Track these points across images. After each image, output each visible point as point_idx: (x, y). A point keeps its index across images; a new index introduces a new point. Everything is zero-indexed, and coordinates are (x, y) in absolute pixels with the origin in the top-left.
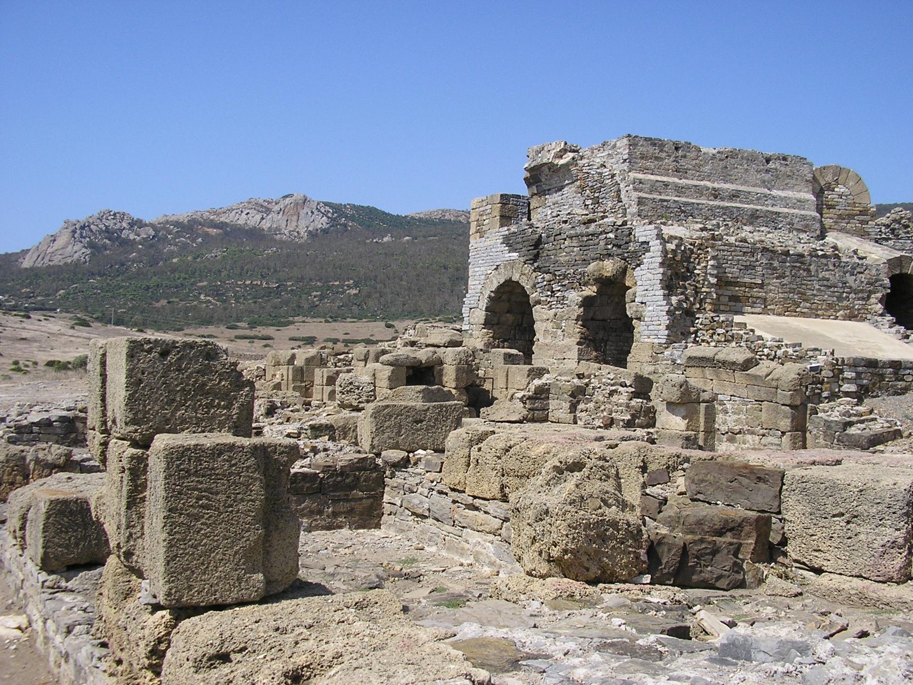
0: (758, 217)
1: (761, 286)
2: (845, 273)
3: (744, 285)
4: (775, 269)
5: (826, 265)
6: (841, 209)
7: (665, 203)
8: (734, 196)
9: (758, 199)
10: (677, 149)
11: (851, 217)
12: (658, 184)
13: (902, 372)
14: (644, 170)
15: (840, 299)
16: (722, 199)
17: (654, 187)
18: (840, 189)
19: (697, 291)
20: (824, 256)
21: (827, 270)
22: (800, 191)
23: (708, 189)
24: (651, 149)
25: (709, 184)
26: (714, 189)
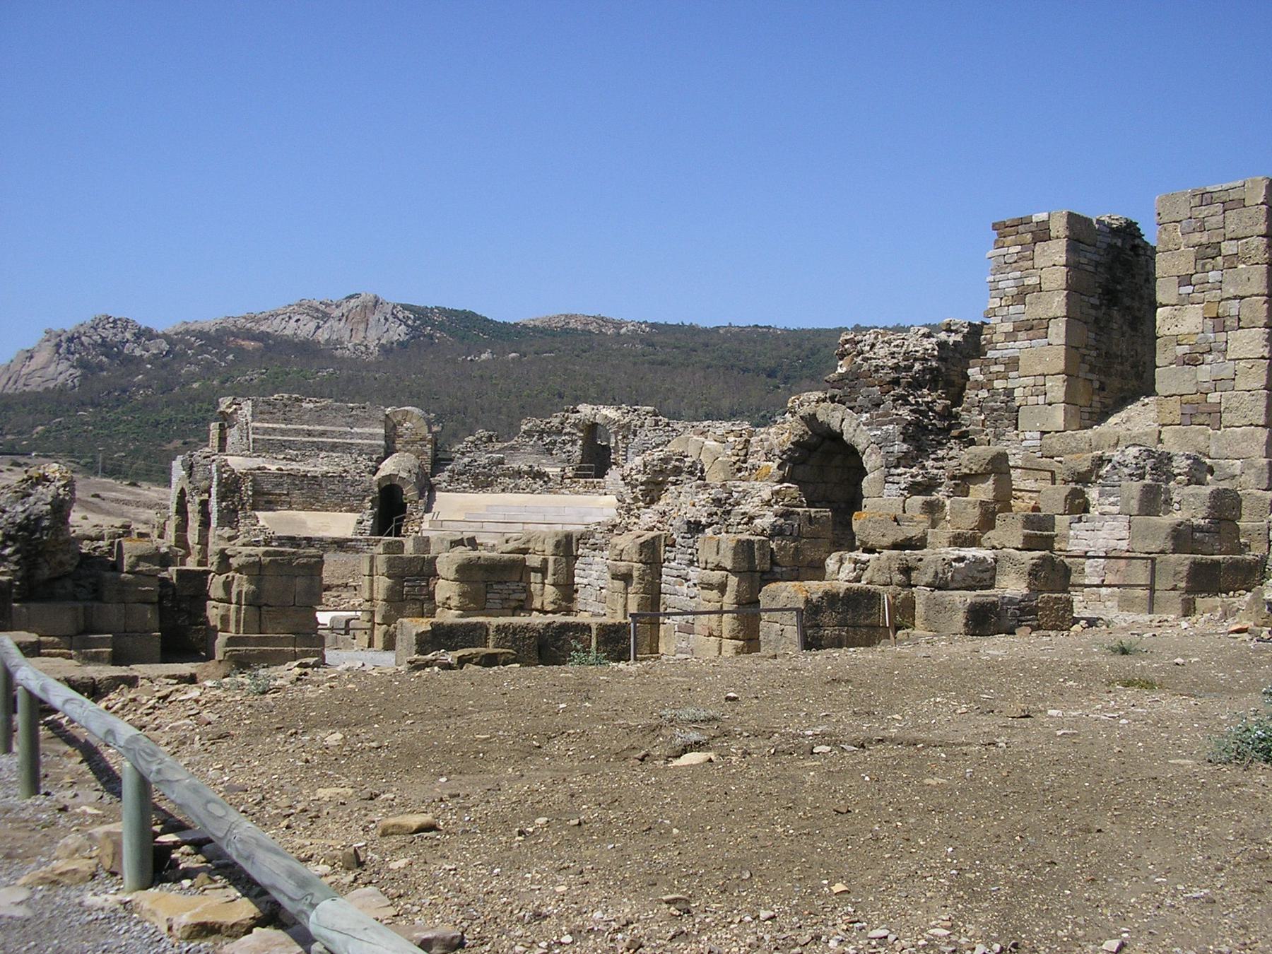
6: (406, 438)
8: (323, 434)
11: (414, 442)
14: (261, 421)
15: (343, 500)
17: (266, 431)
18: (407, 425)
19: (241, 499)
25: (305, 427)
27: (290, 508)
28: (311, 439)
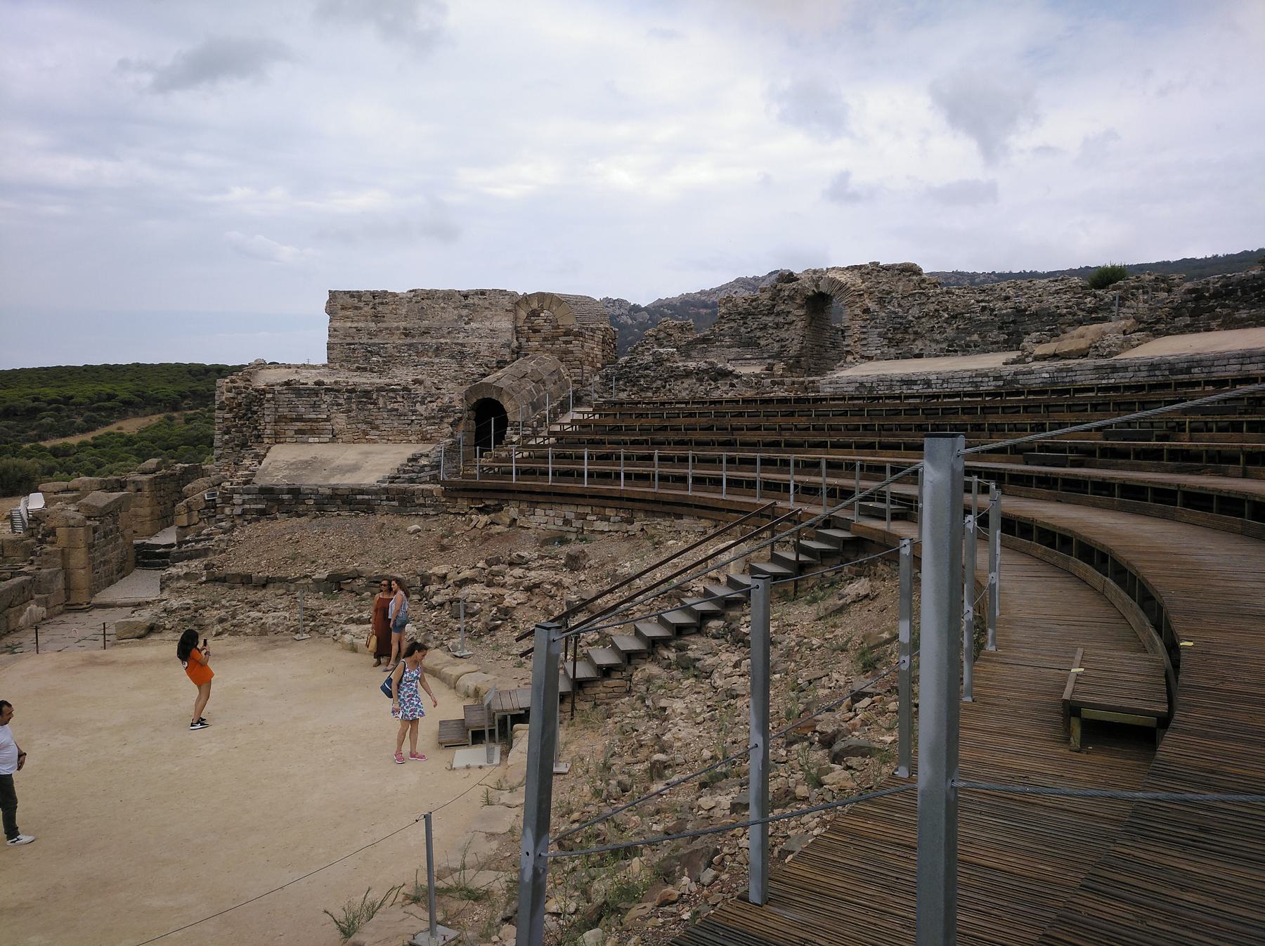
2: (415, 403)
3: (311, 420)
4: (339, 405)
8: (426, 332)
16: (413, 337)
20: (393, 390)
23: (398, 328)
24: (350, 300)
26: (405, 329)
27: (334, 438)
28: (409, 341)
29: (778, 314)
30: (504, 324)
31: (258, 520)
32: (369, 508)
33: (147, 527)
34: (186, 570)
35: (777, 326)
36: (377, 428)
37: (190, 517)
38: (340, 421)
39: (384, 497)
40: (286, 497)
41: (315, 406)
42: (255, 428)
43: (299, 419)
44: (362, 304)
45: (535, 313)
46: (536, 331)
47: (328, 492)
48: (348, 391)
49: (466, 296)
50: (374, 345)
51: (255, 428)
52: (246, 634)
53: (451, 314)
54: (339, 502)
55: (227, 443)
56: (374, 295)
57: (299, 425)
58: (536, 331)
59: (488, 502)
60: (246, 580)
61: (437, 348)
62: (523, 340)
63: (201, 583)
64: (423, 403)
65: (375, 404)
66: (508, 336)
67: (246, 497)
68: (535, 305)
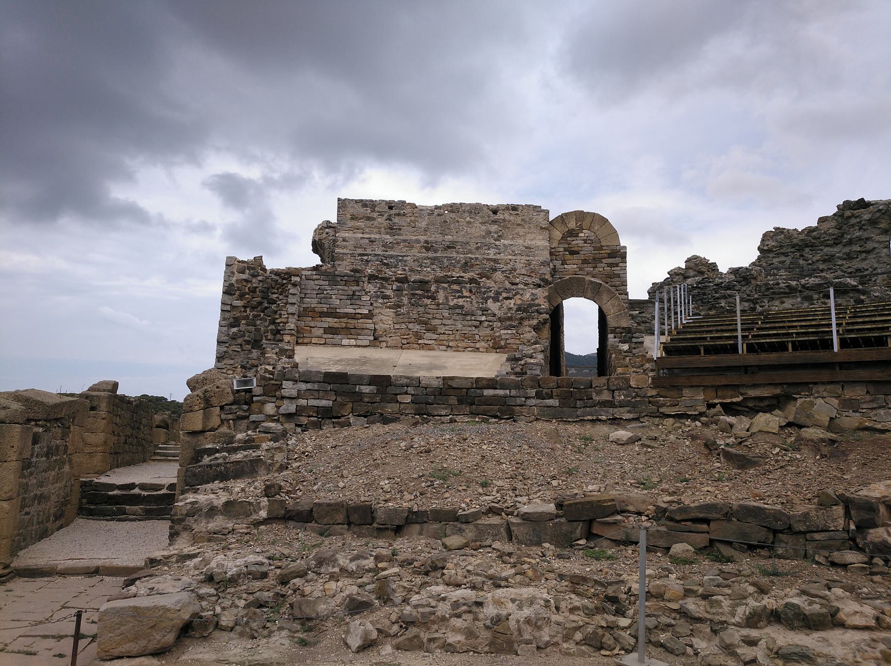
0: (472, 266)
1: (370, 316)
2: (486, 299)
5: (458, 291)
7: (366, 258)
8: (450, 247)
9: (477, 248)
10: (391, 208)
12: (363, 241)
13: (391, 390)
21: (459, 297)
22: (534, 239)
23: (418, 241)
24: (363, 210)
25: (423, 238)
26: (426, 242)
27: (376, 341)
29: (850, 242)
30: (540, 242)
31: (318, 426)
32: (505, 411)
33: (97, 460)
34: (223, 498)
35: (849, 257)
36: (434, 330)
37: (206, 417)
38: (385, 318)
39: (532, 392)
40: (366, 389)
41: (353, 297)
42: (273, 322)
43: (332, 313)
44: (375, 215)
45: (572, 233)
46: (573, 253)
47: (435, 383)
48: (398, 280)
49: (495, 212)
50: (392, 257)
51: (273, 322)
52: (449, 648)
53: (478, 229)
54: (453, 400)
55: (234, 338)
56: (391, 205)
57: (330, 322)
58: (573, 253)
59: (753, 393)
60: (360, 518)
61: (466, 263)
62: (558, 263)
63: (257, 524)
64: (496, 300)
65: (434, 298)
66: (545, 256)
67: (303, 386)
68: (572, 224)
